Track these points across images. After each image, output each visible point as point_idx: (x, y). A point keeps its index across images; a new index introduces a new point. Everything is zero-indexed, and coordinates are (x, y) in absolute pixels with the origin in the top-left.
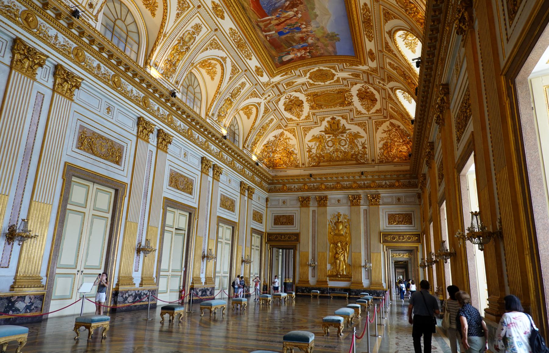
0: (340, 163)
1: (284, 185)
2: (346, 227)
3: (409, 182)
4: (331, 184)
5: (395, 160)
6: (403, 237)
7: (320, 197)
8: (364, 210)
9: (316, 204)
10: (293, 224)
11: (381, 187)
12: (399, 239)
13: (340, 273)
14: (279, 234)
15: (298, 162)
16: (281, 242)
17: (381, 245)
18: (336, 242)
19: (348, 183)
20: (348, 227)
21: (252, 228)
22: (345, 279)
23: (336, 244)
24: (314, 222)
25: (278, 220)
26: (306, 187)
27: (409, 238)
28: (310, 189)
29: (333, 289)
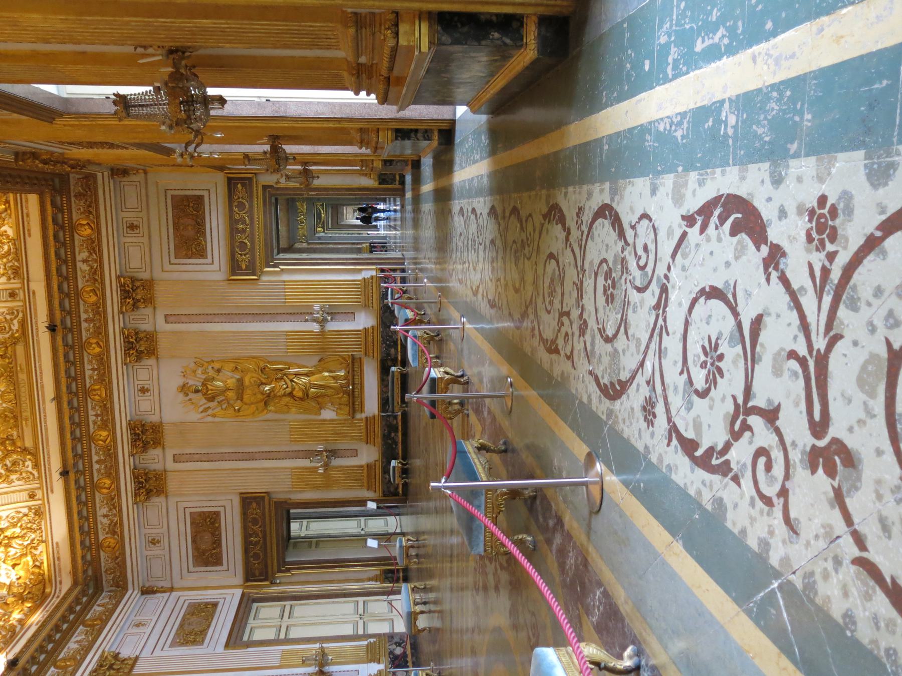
0: (24, 390)
1: (99, 546)
2: (219, 371)
3: (78, 196)
4: (91, 413)
5: (10, 232)
6: (237, 222)
7: (134, 444)
8: (166, 322)
9: (155, 453)
10: (217, 514)
11: (97, 275)
12: (244, 231)
13: (342, 386)
14: (246, 551)
15: (26, 510)
16: (268, 547)
17: (265, 278)
18: (260, 397)
19: (87, 367)
20: (217, 366)
21: (227, 646)
22: (357, 373)
23: (268, 399)
24: (208, 457)
25: (207, 554)
26: (108, 482)
27: (241, 206)
28: (112, 472)
29: (385, 403)
